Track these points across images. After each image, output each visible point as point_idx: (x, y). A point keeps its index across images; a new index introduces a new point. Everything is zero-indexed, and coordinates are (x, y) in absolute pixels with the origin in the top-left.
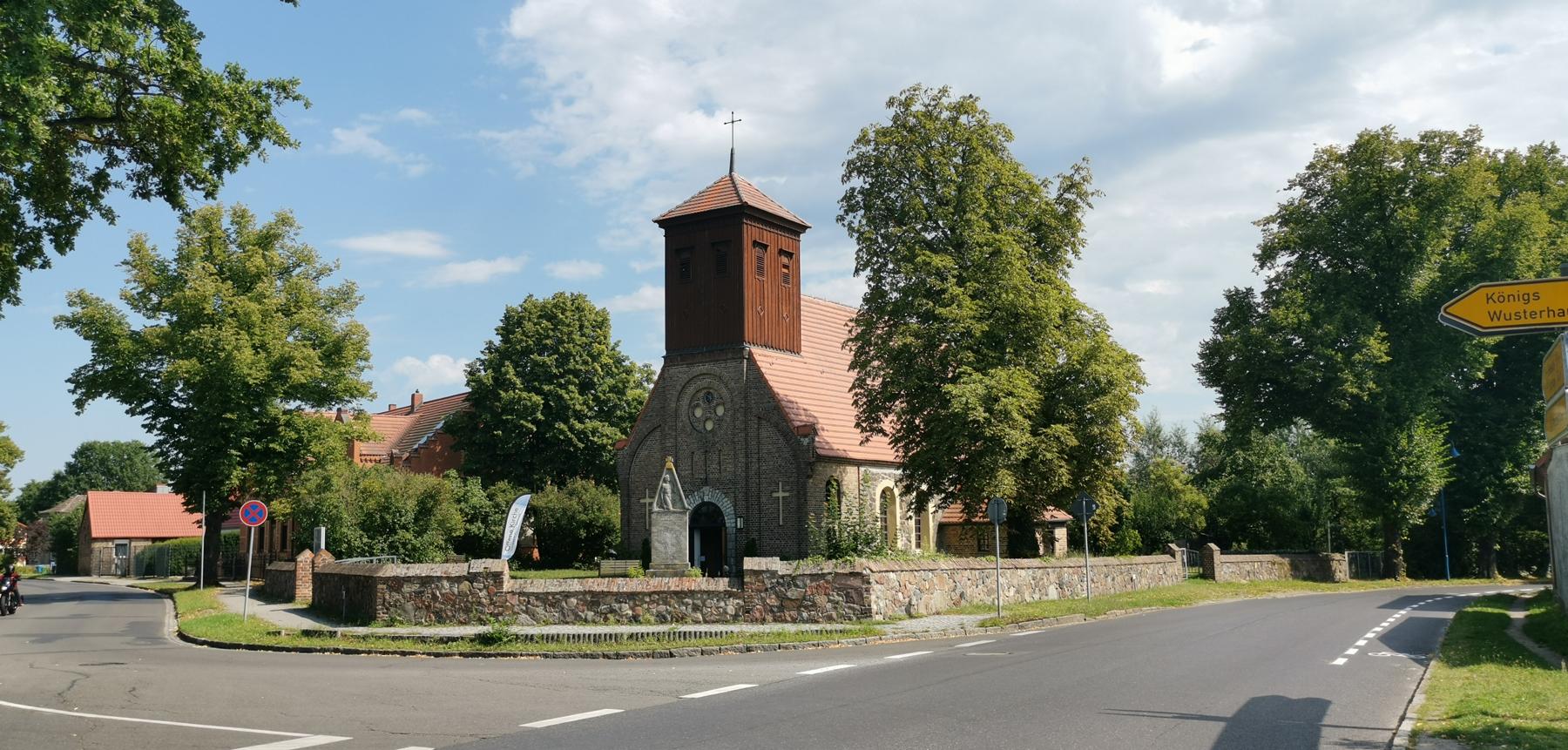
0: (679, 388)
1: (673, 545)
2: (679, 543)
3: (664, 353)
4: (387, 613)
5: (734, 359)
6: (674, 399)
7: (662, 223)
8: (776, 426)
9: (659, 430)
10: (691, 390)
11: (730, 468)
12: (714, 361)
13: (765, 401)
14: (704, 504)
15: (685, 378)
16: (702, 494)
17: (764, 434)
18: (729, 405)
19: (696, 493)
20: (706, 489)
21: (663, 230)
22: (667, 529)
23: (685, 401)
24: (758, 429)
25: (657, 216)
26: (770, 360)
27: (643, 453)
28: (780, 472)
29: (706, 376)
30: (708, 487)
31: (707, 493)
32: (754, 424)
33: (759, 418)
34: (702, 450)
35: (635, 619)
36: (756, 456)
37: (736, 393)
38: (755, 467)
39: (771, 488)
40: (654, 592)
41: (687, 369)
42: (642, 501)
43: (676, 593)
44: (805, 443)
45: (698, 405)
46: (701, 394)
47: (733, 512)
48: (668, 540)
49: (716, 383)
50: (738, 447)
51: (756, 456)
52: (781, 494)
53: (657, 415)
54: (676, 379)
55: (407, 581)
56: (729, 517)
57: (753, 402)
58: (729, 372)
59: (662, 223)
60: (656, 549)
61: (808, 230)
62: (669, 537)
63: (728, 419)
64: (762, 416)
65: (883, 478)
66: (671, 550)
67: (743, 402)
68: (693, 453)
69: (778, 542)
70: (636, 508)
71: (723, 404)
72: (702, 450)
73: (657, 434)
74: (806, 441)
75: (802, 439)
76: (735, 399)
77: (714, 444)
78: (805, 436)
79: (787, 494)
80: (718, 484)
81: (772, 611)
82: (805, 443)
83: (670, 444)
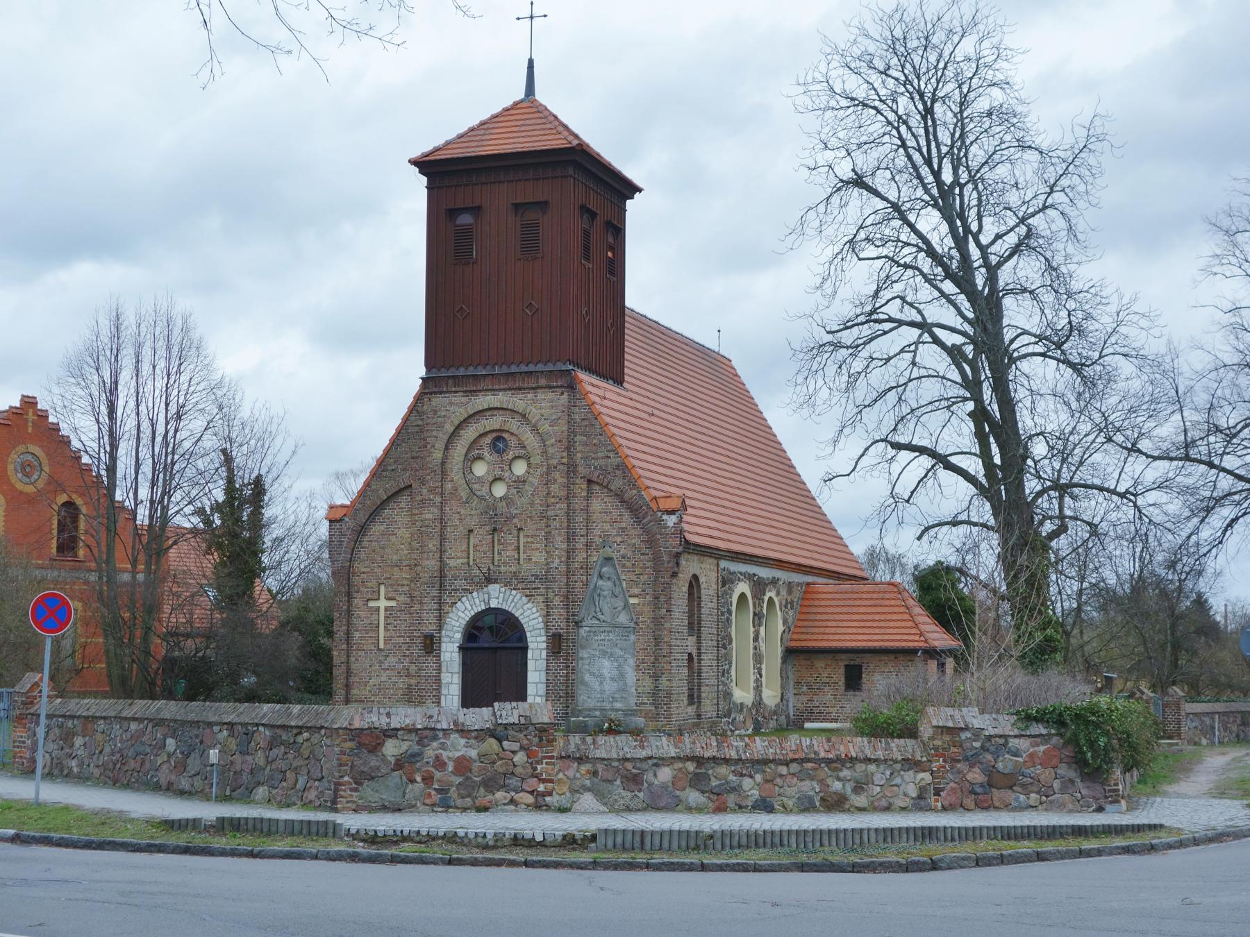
0: (449, 428)
1: (612, 679)
2: (622, 676)
3: (422, 372)
4: (356, 790)
5: (550, 387)
6: (440, 445)
7: (424, 165)
8: (619, 496)
9: (407, 492)
10: (470, 433)
11: (539, 557)
12: (515, 389)
13: (601, 455)
14: (489, 611)
15: (460, 413)
16: (486, 596)
17: (596, 505)
18: (536, 460)
19: (475, 594)
20: (494, 589)
21: (425, 179)
22: (604, 653)
24: (588, 498)
25: (416, 153)
26: (601, 392)
27: (377, 528)
30: (497, 586)
31: (494, 594)
32: (581, 488)
33: (590, 482)
34: (487, 528)
35: (765, 806)
36: (583, 540)
38: (580, 556)
40: (793, 760)
41: (464, 400)
42: (371, 604)
43: (829, 762)
44: (670, 524)
45: (479, 458)
46: (488, 440)
47: (542, 625)
48: (605, 671)
49: (513, 425)
50: (556, 524)
51: (583, 540)
54: (443, 413)
55: (390, 737)
56: (533, 633)
57: (579, 455)
59: (424, 165)
60: (583, 683)
61: (637, 195)
62: (606, 666)
63: (536, 482)
64: (595, 479)
65: (739, 580)
66: (610, 687)
67: (565, 454)
68: (471, 531)
70: (362, 615)
71: (527, 458)
72: (487, 528)
73: (404, 500)
74: (671, 520)
75: (665, 517)
76: (551, 450)
77: (511, 518)
78: (672, 512)
80: (514, 581)
81: (973, 792)
82: (670, 524)
83: (430, 516)
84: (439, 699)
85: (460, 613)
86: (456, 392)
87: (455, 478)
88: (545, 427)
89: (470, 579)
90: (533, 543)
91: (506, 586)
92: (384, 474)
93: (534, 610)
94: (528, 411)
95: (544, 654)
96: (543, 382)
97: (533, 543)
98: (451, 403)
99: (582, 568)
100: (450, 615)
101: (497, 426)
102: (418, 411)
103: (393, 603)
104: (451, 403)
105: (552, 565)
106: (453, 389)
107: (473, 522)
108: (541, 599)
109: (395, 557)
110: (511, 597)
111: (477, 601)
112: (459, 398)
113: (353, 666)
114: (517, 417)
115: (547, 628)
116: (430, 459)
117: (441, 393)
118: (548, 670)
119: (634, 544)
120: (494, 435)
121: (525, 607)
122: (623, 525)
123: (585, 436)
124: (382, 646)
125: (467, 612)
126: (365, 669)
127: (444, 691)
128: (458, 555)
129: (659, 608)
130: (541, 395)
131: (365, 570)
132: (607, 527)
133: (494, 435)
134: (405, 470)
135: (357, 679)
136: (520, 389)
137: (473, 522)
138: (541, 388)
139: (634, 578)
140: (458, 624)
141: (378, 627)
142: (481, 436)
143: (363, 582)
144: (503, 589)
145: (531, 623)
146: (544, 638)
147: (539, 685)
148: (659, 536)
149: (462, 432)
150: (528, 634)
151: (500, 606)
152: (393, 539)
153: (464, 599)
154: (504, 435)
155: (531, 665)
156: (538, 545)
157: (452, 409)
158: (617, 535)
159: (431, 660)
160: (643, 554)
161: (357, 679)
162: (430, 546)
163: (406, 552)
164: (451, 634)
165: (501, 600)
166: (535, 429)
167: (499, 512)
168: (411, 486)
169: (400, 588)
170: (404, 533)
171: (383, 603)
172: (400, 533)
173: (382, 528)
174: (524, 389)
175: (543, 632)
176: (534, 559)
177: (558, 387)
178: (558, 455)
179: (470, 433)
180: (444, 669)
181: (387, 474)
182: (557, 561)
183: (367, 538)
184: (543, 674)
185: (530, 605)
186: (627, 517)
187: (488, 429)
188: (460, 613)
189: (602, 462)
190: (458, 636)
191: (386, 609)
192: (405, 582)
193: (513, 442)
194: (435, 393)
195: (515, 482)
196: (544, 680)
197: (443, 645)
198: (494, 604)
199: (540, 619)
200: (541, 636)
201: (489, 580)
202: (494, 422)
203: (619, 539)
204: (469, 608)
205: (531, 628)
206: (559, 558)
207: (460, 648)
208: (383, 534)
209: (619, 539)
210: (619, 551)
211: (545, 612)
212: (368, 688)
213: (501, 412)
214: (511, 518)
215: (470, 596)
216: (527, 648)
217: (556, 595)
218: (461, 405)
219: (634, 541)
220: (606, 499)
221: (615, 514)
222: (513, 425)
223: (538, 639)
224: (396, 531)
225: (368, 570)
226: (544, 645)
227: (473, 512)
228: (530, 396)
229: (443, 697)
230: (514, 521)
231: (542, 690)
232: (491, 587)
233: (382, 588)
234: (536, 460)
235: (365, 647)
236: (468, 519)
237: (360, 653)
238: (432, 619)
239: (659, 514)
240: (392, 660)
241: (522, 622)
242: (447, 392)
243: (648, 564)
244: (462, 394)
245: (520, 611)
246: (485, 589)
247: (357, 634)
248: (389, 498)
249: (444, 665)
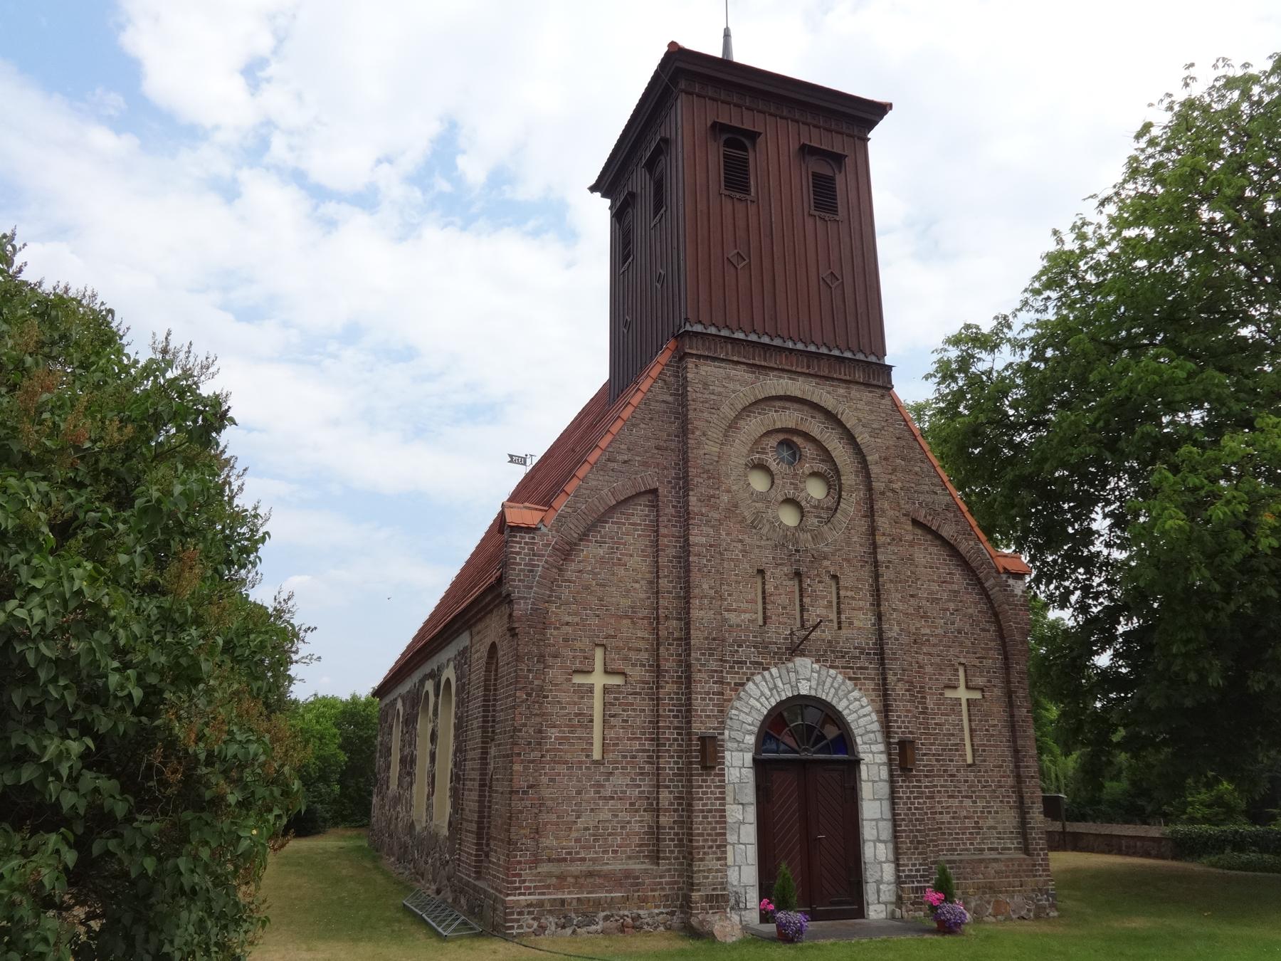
5: (867, 385)
6: (716, 433)
9: (644, 500)
10: (754, 426)
18: (849, 478)
19: (774, 671)
20: (804, 664)
23: (738, 450)
27: (591, 551)
28: (961, 644)
29: (788, 404)
30: (807, 661)
37: (876, 457)
39: (944, 679)
41: (749, 377)
42: (578, 679)
44: (1018, 591)
46: (773, 441)
47: (876, 726)
49: (815, 427)
52: (962, 694)
53: (645, 464)
54: (718, 390)
56: (866, 738)
58: (857, 409)
69: (968, 802)
73: (640, 512)
75: (1011, 582)
76: (875, 470)
79: (977, 695)
80: (829, 655)
82: (1018, 591)
84: (725, 852)
85: (752, 702)
86: (738, 363)
87: (734, 488)
88: (863, 437)
89: (762, 647)
90: (853, 598)
91: (818, 661)
92: (611, 465)
93: (865, 701)
94: (841, 410)
95: (884, 773)
96: (859, 376)
97: (853, 598)
98: (728, 378)
99: (915, 642)
100: (737, 704)
101: (791, 425)
102: (665, 381)
103: (617, 680)
104: (728, 378)
105: (890, 634)
106: (735, 358)
107: (765, 557)
108: (870, 685)
109: (625, 602)
110: (829, 680)
111: (780, 684)
112: (740, 373)
113: (546, 793)
114: (820, 416)
115: (887, 730)
116: (702, 452)
117: (714, 359)
118: (893, 798)
119: (971, 616)
120: (781, 437)
121: (851, 696)
122: (955, 587)
123: (903, 459)
124: (597, 755)
125: (762, 700)
126: (570, 798)
127: (731, 838)
128: (744, 606)
129: (1019, 707)
130: (855, 392)
131: (569, 619)
132: (935, 587)
133: (781, 437)
134: (645, 464)
135: (554, 817)
136: (827, 378)
137: (765, 557)
138: (857, 383)
139: (977, 662)
140: (750, 720)
141: (592, 721)
142: (769, 433)
143: (566, 640)
144: (816, 666)
145: (862, 721)
146: (881, 747)
147: (881, 824)
148: (1007, 607)
149: (741, 423)
150: (859, 740)
151: (813, 693)
152: (621, 572)
153: (758, 678)
154: (795, 439)
155: (866, 790)
156: (861, 603)
157: (731, 386)
158: (949, 601)
159: (712, 780)
160: (983, 630)
161: (554, 817)
162: (705, 586)
163: (643, 596)
164: (738, 736)
165: (814, 683)
166: (850, 437)
167: (801, 546)
168: (654, 492)
169: (632, 655)
170: (638, 563)
171: (598, 680)
172: (631, 562)
173: (601, 552)
174: (833, 379)
175: (879, 737)
176: (856, 623)
177: (878, 387)
178: (885, 478)
179: (754, 426)
180: (729, 799)
181: (615, 465)
182: (896, 628)
183: (573, 566)
184: (886, 805)
185: (856, 694)
186: (959, 580)
187: (779, 425)
188: (752, 702)
189: (929, 498)
190: (751, 740)
191: (606, 689)
192: (642, 645)
193: (808, 450)
194: (706, 357)
195: (815, 507)
196: (888, 815)
197: (727, 754)
198: (804, 691)
199: (874, 717)
200: (876, 742)
201: (795, 650)
202: (789, 418)
203: (952, 606)
204: (768, 693)
205: (861, 731)
206: (899, 624)
207: (754, 760)
208: (602, 561)
209: (952, 606)
210: (953, 623)
211: (879, 705)
212: (574, 835)
213: (796, 406)
214: (817, 559)
215: (766, 673)
216: (857, 762)
217: (899, 680)
218: (744, 383)
219: (970, 611)
220: (931, 549)
221: (944, 571)
222: (815, 427)
223: (874, 748)
224: (625, 558)
225: (577, 619)
226: (883, 758)
227: (763, 543)
228: (841, 391)
229: (729, 848)
230: (826, 563)
231: (886, 830)
232: (799, 661)
233: (599, 653)
234: (849, 478)
235: (568, 757)
236: (757, 551)
237: (562, 769)
238: (711, 709)
239: (1004, 577)
240: (619, 781)
241: (849, 719)
242: (723, 360)
243: (993, 644)
244: (744, 367)
245: (844, 703)
246: (790, 665)
247: (553, 733)
248: (619, 503)
249: (729, 789)
